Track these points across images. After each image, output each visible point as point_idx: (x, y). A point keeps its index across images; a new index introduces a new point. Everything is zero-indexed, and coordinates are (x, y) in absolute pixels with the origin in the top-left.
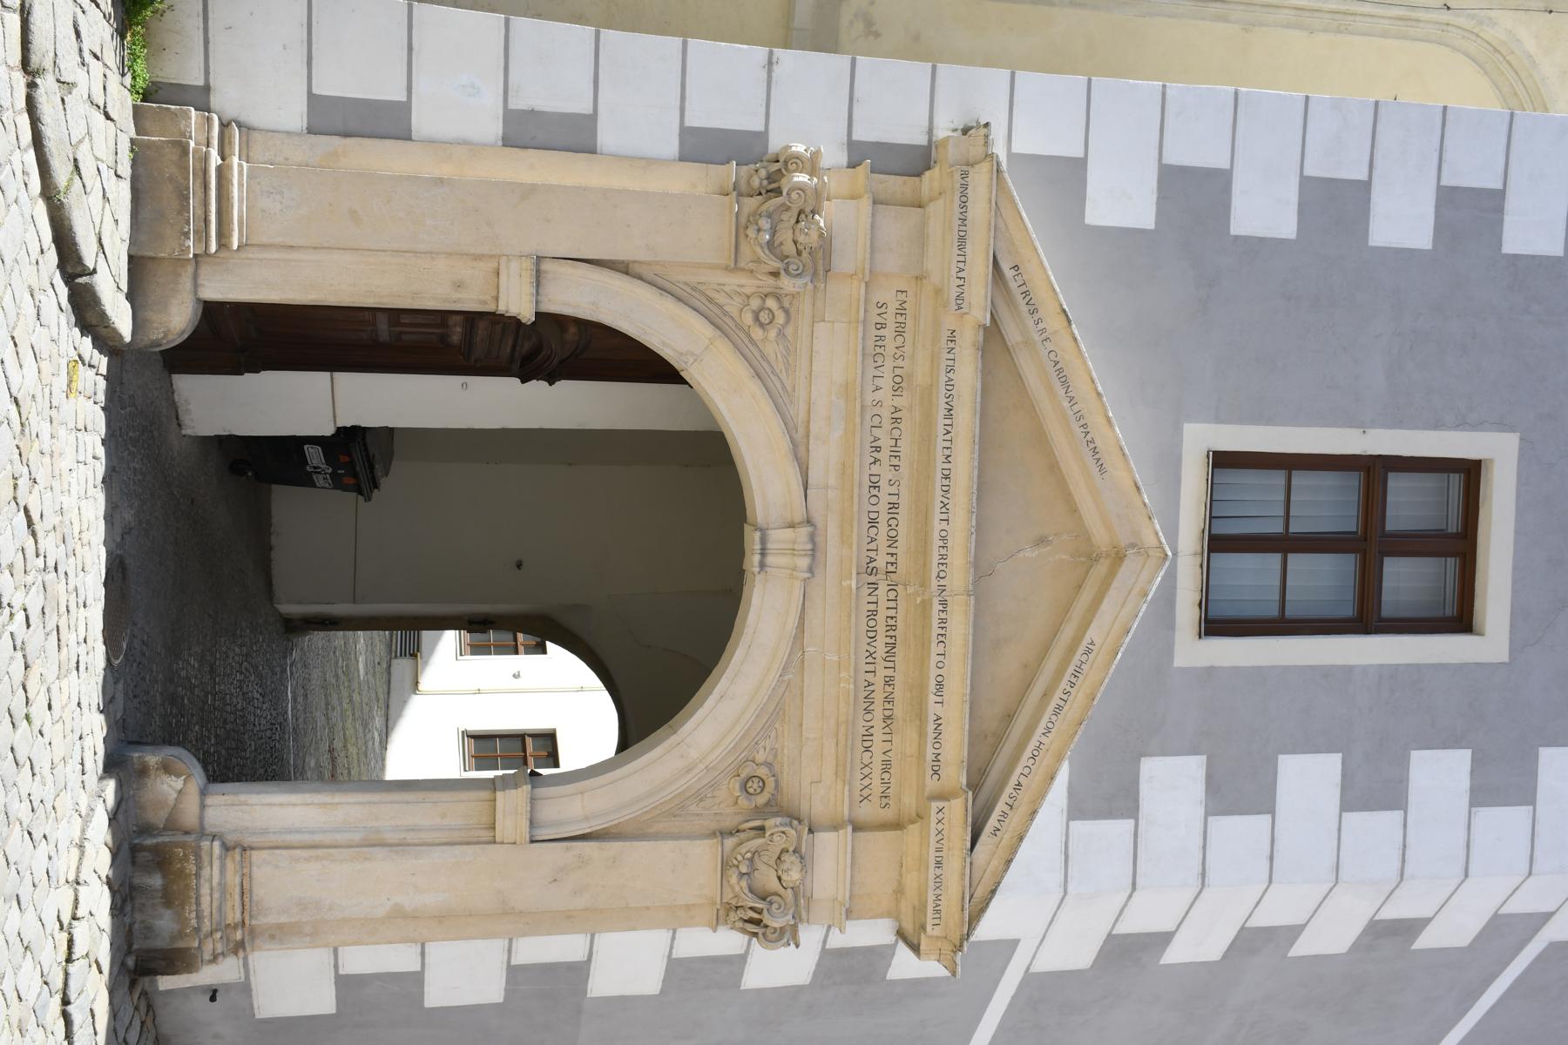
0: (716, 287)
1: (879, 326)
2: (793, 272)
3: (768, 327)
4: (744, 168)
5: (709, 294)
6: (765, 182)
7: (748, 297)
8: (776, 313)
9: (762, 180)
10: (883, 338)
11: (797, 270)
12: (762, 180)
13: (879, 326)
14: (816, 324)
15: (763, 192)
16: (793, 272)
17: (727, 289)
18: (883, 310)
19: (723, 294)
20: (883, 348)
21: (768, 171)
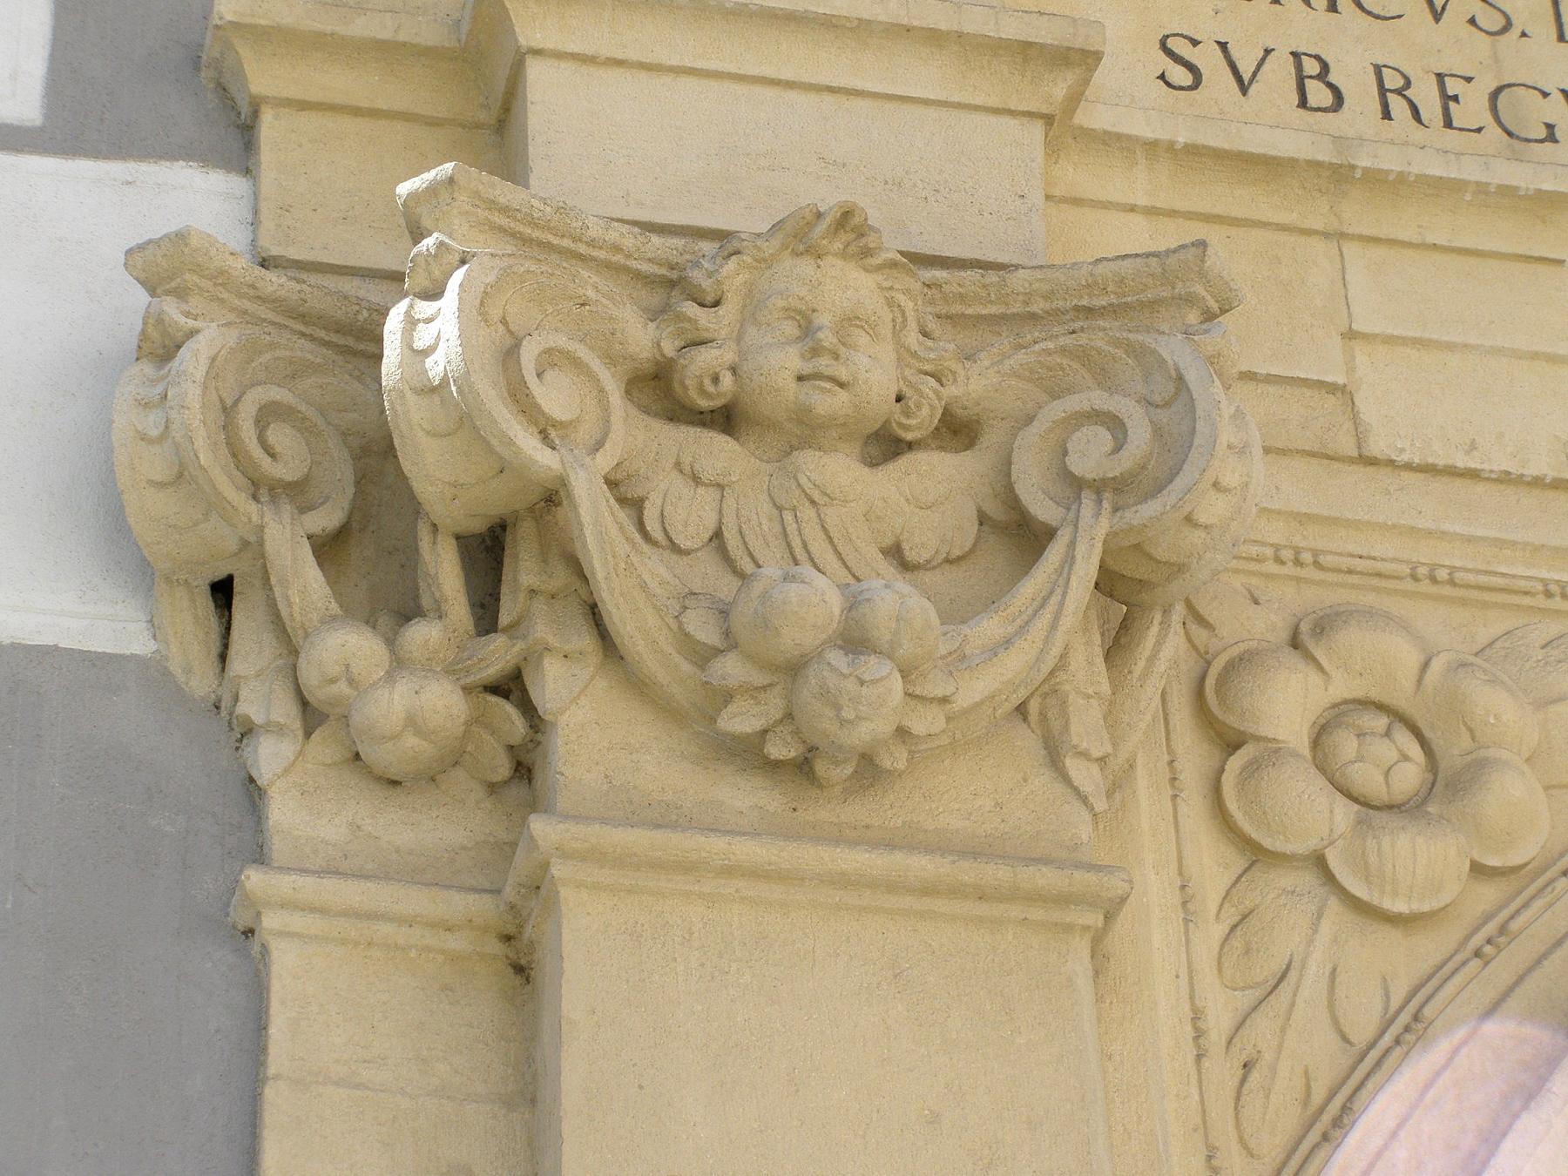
0: (1222, 1072)
1: (1318, 94)
2: (1140, 435)
3: (1453, 749)
4: (283, 812)
5: (1289, 1122)
6: (422, 635)
7: (1256, 855)
8: (1342, 687)
9: (399, 663)
10: (1392, 81)
11: (1116, 425)
12: (399, 663)
13: (1318, 94)
14: (1378, 446)
15: (497, 655)
16: (1140, 435)
17: (1220, 1016)
18: (1208, 60)
19: (1263, 1029)
20: (1453, 87)
21: (330, 621)
